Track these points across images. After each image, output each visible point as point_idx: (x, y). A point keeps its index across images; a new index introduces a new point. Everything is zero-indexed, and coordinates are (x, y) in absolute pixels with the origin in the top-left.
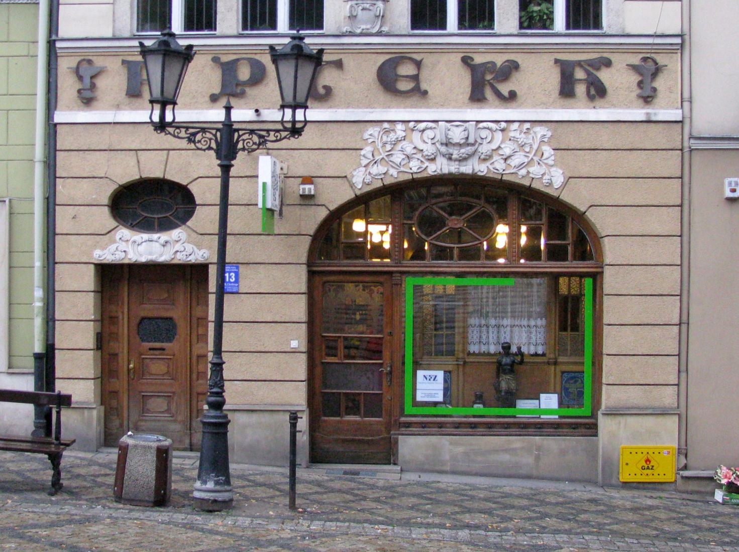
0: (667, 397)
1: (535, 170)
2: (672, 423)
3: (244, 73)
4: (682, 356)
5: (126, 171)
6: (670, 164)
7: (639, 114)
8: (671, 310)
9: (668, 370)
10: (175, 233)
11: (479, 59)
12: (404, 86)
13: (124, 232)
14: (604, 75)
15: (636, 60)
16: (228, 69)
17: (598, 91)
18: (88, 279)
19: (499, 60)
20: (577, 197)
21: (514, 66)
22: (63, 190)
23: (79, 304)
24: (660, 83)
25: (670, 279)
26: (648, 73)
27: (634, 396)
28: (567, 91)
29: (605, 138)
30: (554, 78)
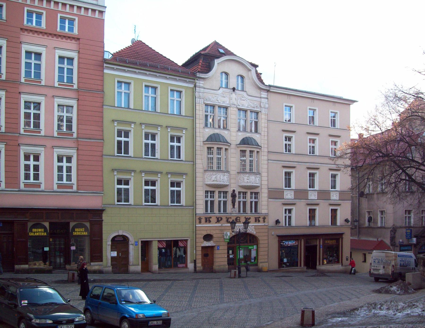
0: (266, 260)
1: (253, 232)
2: (267, 264)
3: (220, 219)
4: (268, 255)
5: (205, 233)
6: (266, 231)
7: (263, 224)
8: (267, 249)
9: (266, 257)
10: (212, 242)
11: (247, 217)
12: (238, 221)
13: (205, 242)
14: (260, 219)
15: (263, 217)
16: (218, 218)
17: (259, 221)
18: (200, 249)
19: (249, 217)
20: (257, 235)
21: (250, 218)
22: (197, 236)
23: (199, 253)
24: (266, 220)
25: (267, 245)
26: (264, 218)
27: (263, 261)
28: (256, 221)
29: (260, 227)
30: (254, 220)
